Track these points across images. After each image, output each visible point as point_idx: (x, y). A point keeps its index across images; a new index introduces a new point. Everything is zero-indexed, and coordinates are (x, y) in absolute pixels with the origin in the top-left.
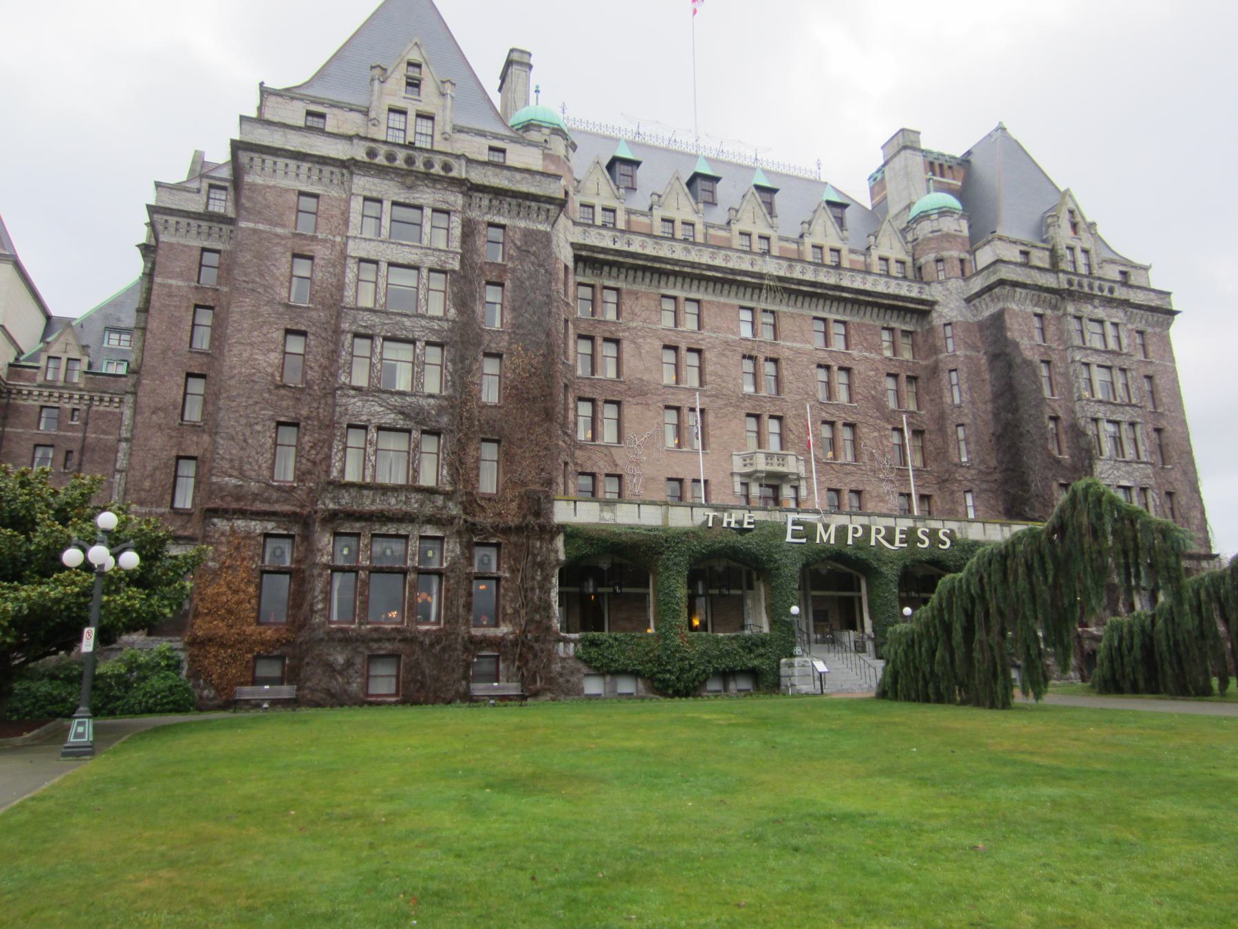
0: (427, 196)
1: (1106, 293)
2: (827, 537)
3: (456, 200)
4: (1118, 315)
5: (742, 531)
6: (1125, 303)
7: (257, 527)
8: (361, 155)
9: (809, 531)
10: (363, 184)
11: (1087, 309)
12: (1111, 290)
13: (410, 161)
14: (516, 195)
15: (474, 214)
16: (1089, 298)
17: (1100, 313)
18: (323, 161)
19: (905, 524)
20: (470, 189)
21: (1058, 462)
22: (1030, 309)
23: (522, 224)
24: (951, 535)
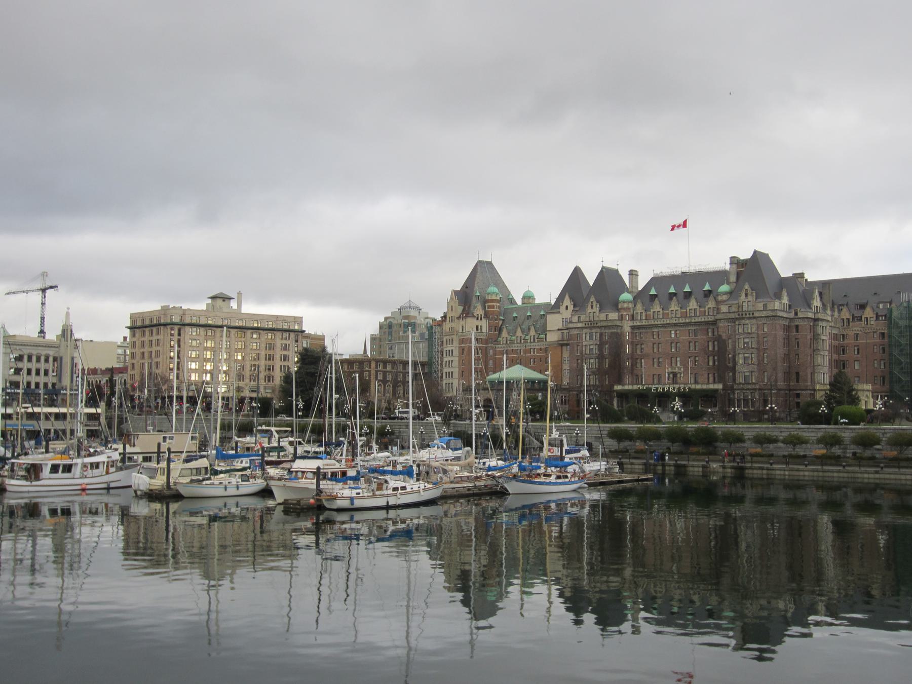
0: (594, 330)
1: (751, 316)
2: (660, 390)
3: (598, 330)
4: (754, 321)
5: (643, 390)
6: (755, 318)
7: (575, 392)
8: (584, 325)
9: (657, 388)
10: (585, 331)
11: (743, 322)
12: (753, 314)
13: (591, 324)
14: (608, 326)
15: (602, 331)
16: (743, 318)
17: (747, 322)
18: (579, 328)
19: (682, 386)
20: (600, 327)
21: (728, 366)
22: (726, 324)
23: (610, 331)
24: (689, 388)
